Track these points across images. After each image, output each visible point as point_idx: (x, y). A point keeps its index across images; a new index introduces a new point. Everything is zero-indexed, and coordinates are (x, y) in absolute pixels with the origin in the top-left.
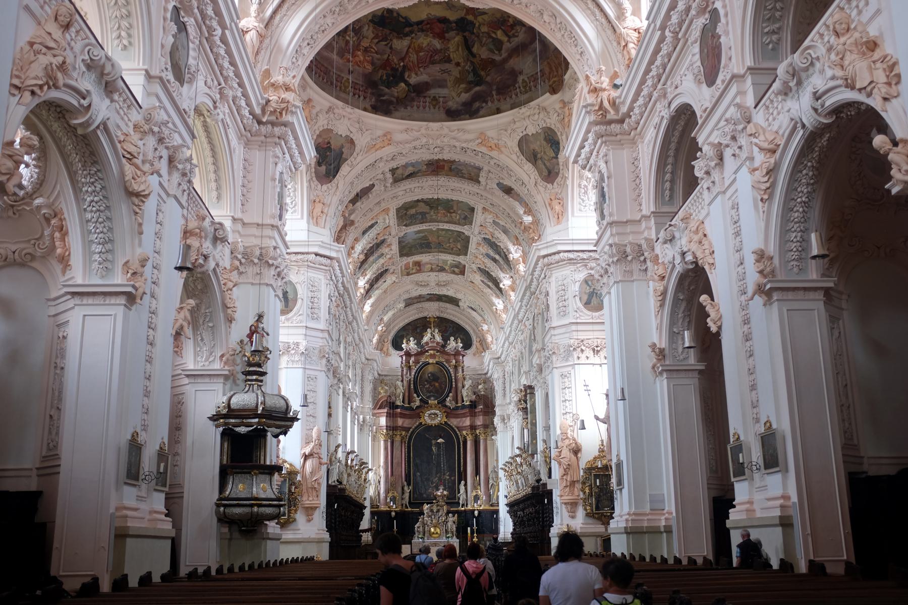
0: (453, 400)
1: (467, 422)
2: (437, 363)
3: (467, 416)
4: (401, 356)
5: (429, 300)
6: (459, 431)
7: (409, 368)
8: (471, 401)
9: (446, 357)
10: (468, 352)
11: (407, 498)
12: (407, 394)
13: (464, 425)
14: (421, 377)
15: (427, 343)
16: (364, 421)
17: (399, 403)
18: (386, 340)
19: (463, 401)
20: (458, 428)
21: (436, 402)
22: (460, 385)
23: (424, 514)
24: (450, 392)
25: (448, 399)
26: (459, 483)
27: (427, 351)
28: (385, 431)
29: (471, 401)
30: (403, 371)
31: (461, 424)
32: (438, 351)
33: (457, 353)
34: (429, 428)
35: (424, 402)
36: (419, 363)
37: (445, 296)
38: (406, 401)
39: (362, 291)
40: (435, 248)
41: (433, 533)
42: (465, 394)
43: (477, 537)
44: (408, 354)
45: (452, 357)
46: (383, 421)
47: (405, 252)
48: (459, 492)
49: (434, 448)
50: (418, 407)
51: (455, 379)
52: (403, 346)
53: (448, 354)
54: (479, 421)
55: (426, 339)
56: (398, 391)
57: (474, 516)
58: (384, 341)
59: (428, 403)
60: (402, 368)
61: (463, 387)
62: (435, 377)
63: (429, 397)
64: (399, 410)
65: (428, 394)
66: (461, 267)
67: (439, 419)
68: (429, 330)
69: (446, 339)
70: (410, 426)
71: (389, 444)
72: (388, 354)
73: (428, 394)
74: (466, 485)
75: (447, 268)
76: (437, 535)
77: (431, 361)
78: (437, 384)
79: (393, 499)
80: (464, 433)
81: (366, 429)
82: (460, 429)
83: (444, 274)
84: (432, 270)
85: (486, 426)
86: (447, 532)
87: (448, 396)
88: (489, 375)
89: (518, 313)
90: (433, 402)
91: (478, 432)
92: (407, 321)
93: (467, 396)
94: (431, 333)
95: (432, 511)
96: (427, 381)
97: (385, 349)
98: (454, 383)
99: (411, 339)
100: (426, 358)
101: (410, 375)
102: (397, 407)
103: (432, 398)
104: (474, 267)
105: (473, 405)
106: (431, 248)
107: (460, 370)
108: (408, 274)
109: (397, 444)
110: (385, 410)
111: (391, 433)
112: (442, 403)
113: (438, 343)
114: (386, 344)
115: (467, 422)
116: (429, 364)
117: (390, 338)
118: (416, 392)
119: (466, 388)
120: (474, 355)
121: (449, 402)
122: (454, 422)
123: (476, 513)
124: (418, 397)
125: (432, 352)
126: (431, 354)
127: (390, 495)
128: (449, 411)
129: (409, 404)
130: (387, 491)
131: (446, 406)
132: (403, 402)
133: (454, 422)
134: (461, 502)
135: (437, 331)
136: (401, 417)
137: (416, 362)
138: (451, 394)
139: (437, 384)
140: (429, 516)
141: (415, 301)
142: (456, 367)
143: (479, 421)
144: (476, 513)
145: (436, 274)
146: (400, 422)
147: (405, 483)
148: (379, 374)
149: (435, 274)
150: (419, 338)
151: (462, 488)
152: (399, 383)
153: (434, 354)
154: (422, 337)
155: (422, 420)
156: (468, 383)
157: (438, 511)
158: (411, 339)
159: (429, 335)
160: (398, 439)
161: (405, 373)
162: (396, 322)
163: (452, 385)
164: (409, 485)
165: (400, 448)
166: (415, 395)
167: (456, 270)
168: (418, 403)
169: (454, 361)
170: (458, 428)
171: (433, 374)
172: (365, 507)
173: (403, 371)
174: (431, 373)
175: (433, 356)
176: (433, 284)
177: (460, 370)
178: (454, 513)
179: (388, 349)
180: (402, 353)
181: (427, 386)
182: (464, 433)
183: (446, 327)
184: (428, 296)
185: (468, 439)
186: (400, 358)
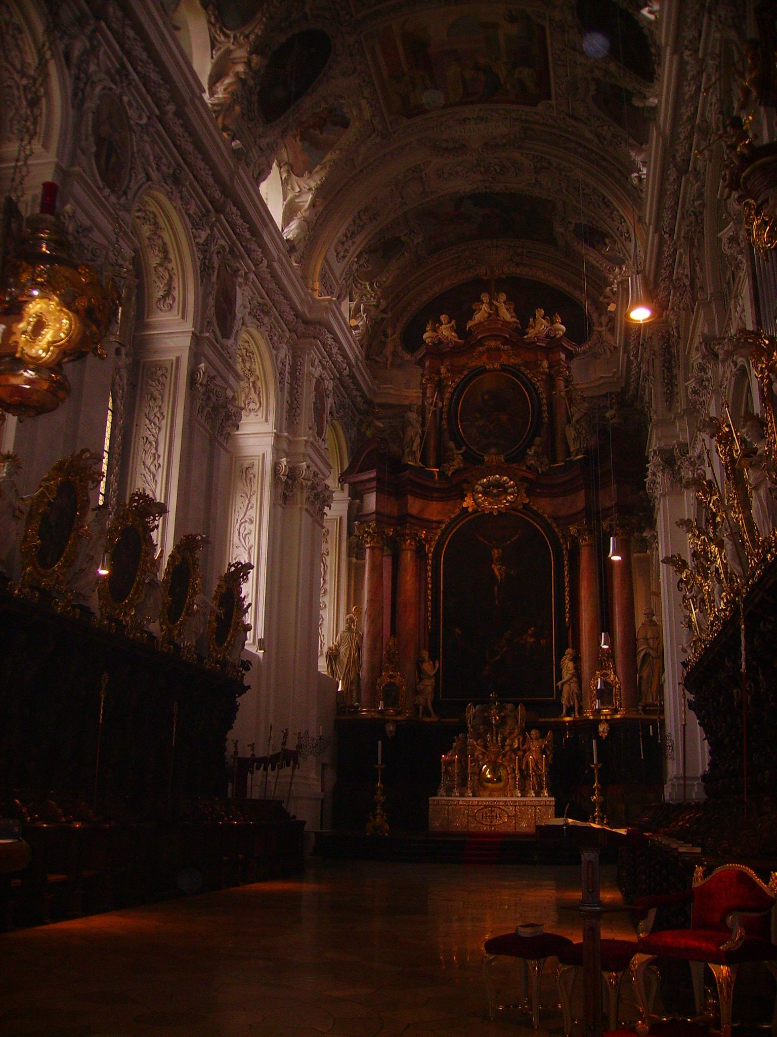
1: (580, 501)
2: (504, 369)
4: (421, 363)
7: (440, 387)
11: (429, 689)
16: (292, 473)
18: (389, 331)
19: (568, 453)
21: (502, 458)
23: (466, 731)
26: (560, 655)
27: (480, 343)
28: (373, 524)
32: (506, 342)
33: (552, 344)
34: (480, 518)
39: (240, 68)
41: (489, 780)
42: (571, 433)
43: (602, 792)
46: (371, 502)
48: (559, 677)
49: (496, 569)
50: (457, 471)
51: (550, 405)
52: (425, 336)
54: (608, 499)
55: (478, 317)
56: (410, 432)
57: (599, 738)
58: (386, 336)
59: (482, 462)
68: (485, 298)
69: (524, 315)
71: (387, 562)
74: (576, 660)
76: (501, 785)
79: (391, 695)
81: (301, 497)
86: (524, 777)
87: (529, 445)
94: (491, 304)
95: (486, 722)
103: (493, 450)
107: (561, 384)
110: (372, 474)
113: (505, 322)
115: (580, 501)
116: (484, 370)
123: (603, 728)
125: (493, 344)
126: (489, 350)
127: (385, 679)
130: (376, 670)
132: (424, 459)
134: (564, 701)
135: (503, 297)
138: (538, 440)
140: (478, 736)
142: (551, 381)
143: (608, 499)
144: (603, 728)
146: (414, 506)
147: (425, 655)
148: (368, 402)
150: (461, 315)
151: (568, 666)
153: (498, 349)
154: (470, 315)
155: (468, 502)
157: (503, 721)
159: (485, 307)
164: (433, 657)
166: (452, 445)
168: (458, 463)
169: (545, 364)
170: (556, 519)
172: (244, 689)
177: (561, 384)
178: (543, 730)
180: (422, 352)
182: (573, 530)
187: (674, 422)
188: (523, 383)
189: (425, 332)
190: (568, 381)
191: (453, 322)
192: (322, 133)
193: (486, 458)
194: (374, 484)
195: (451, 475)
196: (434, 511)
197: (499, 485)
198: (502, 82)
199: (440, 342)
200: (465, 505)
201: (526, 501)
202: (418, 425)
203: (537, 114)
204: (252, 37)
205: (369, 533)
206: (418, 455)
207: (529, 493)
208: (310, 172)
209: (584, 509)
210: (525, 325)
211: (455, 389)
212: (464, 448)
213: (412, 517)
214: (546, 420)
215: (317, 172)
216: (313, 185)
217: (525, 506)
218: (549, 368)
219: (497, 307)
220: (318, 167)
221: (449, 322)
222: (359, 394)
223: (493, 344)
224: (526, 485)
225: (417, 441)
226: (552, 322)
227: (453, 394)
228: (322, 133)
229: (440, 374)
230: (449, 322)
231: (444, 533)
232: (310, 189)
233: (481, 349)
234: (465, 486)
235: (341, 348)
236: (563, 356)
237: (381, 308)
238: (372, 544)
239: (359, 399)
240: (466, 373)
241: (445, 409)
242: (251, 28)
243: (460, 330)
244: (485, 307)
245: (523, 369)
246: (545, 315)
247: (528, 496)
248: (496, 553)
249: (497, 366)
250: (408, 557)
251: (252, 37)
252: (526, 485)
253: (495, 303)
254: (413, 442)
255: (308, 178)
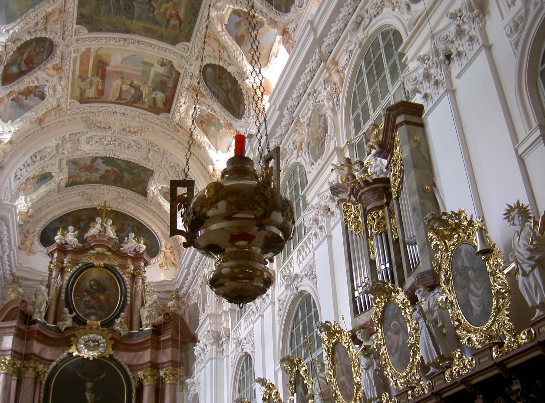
0: (126, 323)
1: (147, 356)
2: (106, 267)
3: (147, 348)
4: (51, 254)
5: (104, 180)
6: (131, 371)
7: (62, 271)
8: (154, 326)
9: (120, 261)
10: (153, 261)
12: (53, 308)
13: (141, 362)
14: (79, 285)
15: (93, 236)
17: (39, 318)
18: (31, 231)
20: (130, 366)
21: (99, 323)
22: (138, 302)
24: (122, 310)
25: (118, 321)
27: (92, 248)
28: (8, 358)
29: (154, 326)
30: (51, 275)
31: (135, 362)
32: (109, 250)
33: (137, 257)
35: (79, 321)
36: (77, 264)
37: (130, 166)
38: (51, 319)
40: (139, 19)
42: (145, 313)
44: (63, 249)
45: (129, 262)
47: (85, 11)
49: (88, 395)
50: (67, 329)
52: (56, 238)
53: (124, 256)
55: (93, 231)
56: (40, 298)
58: (28, 231)
59: (85, 324)
60: (51, 270)
61: (143, 305)
62: (100, 287)
63: (88, 315)
64: (37, 326)
65: (88, 311)
66: (170, 84)
67: (101, 349)
68: (99, 220)
70: (52, 358)
71: (14, 383)
72: (31, 252)
73: (88, 311)
75: (145, 91)
77: (96, 263)
78: (102, 297)
80: (140, 374)
82: (134, 368)
83: (136, 111)
84: (120, 100)
85: (174, 364)
87: (118, 316)
88: (183, 291)
89: (324, 34)
90: (93, 322)
91: (162, 373)
92: (66, 210)
93: (148, 317)
94: (102, 225)
96: (87, 291)
97: (28, 243)
98: (129, 299)
99: (71, 228)
100: (90, 258)
101: (62, 280)
102: (35, 322)
103: (93, 317)
104: (195, 69)
105: (157, 330)
106: (132, 18)
108: (83, 100)
109: (28, 383)
110: (14, 323)
111: (19, 363)
112: (108, 324)
113: (110, 239)
114: (30, 236)
115: (147, 356)
116: (93, 266)
117: (39, 228)
118: (68, 304)
119: (147, 305)
120: (161, 266)
121: (120, 325)
122: (124, 358)
124: (71, 312)
125: (100, 249)
126: (98, 253)
128: (118, 338)
129: (55, 323)
131: (114, 331)
132: (46, 317)
133: (124, 358)
135: (110, 222)
136: (39, 341)
137: (74, 263)
139: (102, 297)
141: (84, 175)
142: (133, 277)
145: (128, 109)
146: (37, 347)
148: (12, 274)
149: (123, 107)
152: (44, 288)
153: (103, 254)
156: (150, 300)
158: (71, 228)
159: (98, 226)
160: (30, 374)
161: (53, 276)
162: (51, 208)
163: (125, 300)
165: (31, 389)
166: (66, 310)
167: (160, 96)
168: (69, 322)
169: (132, 267)
170: (130, 366)
171: (98, 282)
173: (51, 275)
174: (94, 280)
175: (99, 256)
176: (117, 128)
179: (32, 244)
180: (53, 247)
181: (87, 299)
182: (140, 374)
183: (123, 225)
184: (103, 168)
185: (146, 383)
186: (50, 259)
187: (221, 315)
188: (117, 277)
189: (57, 235)
190: (143, 280)
191: (77, 232)
192: (26, 99)
193: (88, 321)
194: (13, 330)
195: (65, 330)
196: (48, 353)
197: (94, 341)
198: (144, 97)
199: (66, 243)
200: (71, 351)
201: (112, 352)
202: (46, 295)
203: (158, 119)
204: (11, 32)
205: (5, 364)
206: (44, 314)
207: (114, 348)
208: (13, 121)
209: (150, 361)
210: (121, 240)
211: (73, 274)
212: (74, 314)
213: (35, 355)
214: (129, 302)
215: (17, 122)
216: (12, 130)
217: (111, 356)
218: (134, 270)
219: (105, 228)
220: (18, 119)
221: (74, 232)
222: (9, 268)
223: (100, 249)
224: (113, 342)
225: (45, 305)
226: (138, 242)
227: (71, 278)
228: (26, 99)
229: (63, 263)
230: (74, 232)
231: (55, 368)
232: (10, 132)
233: (92, 251)
234: (72, 339)
235: (9, 237)
236: (142, 264)
237: (29, 214)
238: (6, 371)
239: (8, 272)
240: (80, 265)
241: (65, 286)
242: (11, 27)
243: (80, 238)
244: (98, 226)
245: (117, 268)
246: (135, 237)
247: (113, 349)
248: (89, 385)
249: (102, 264)
250: (28, 383)
251: (11, 32)
252: (113, 342)
253: (105, 225)
254: (41, 306)
255: (11, 125)
